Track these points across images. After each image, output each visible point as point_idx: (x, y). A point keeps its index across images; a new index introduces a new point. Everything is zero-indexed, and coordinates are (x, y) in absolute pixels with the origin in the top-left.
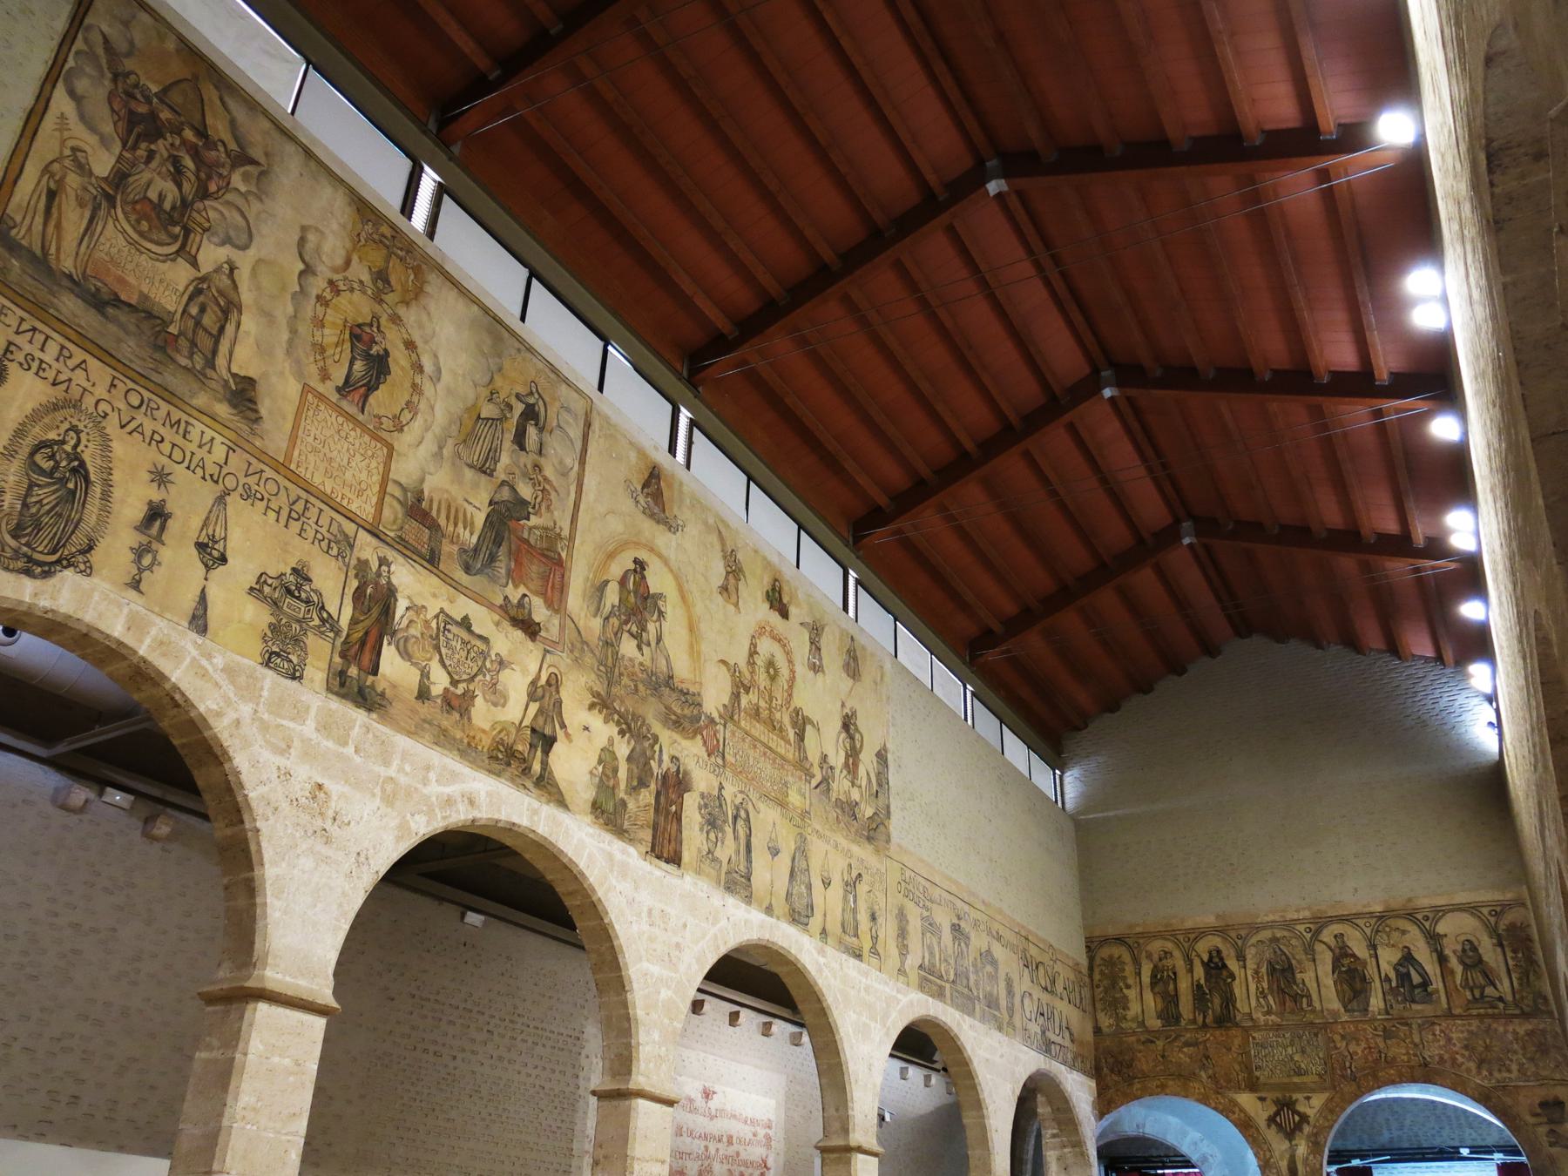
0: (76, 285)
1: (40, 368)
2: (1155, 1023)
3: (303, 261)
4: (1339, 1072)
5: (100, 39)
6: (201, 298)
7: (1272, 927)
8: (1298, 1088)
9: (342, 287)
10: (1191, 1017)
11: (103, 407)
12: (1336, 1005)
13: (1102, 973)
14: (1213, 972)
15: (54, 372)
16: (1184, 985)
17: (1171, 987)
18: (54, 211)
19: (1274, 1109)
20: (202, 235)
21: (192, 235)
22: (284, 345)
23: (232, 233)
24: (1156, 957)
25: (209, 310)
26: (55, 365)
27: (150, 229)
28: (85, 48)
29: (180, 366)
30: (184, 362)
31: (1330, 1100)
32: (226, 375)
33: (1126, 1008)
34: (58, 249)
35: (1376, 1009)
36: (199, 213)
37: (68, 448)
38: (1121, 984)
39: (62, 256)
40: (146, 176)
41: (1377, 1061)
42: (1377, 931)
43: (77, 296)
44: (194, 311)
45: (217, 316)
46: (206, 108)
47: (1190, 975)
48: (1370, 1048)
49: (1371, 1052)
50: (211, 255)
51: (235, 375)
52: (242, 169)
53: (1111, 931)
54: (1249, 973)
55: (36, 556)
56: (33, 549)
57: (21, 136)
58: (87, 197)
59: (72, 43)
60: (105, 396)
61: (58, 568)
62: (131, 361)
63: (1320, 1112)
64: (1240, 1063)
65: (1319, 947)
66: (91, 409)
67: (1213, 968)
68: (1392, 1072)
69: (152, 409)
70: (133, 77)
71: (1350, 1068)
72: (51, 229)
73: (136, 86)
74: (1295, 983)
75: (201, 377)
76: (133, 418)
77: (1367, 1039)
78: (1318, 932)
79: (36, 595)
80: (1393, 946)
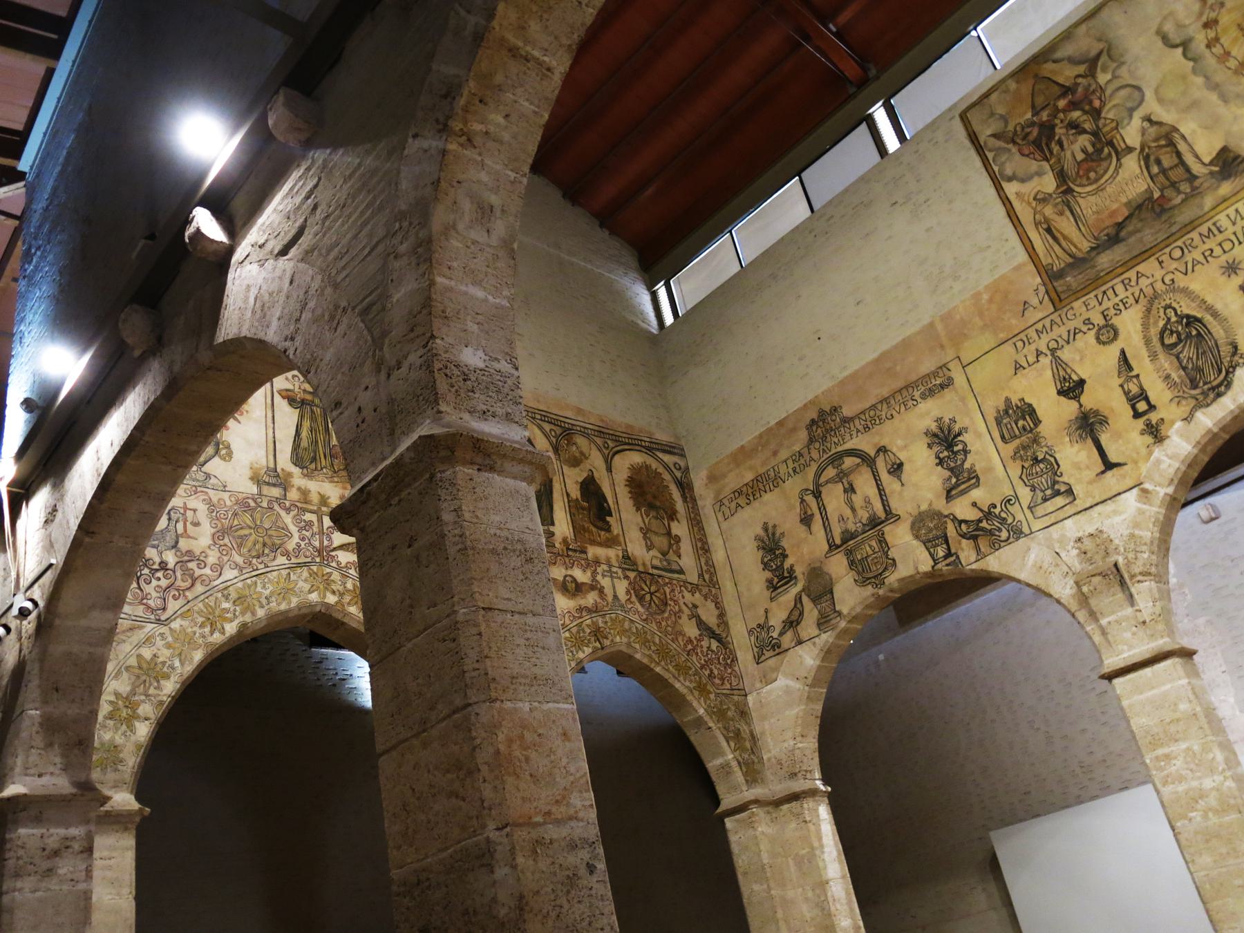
0: (1097, 249)
1: (1124, 304)
3: (1176, 46)
5: (992, 139)
6: (1152, 158)
9: (1213, 15)
11: (1167, 280)
15: (1131, 297)
18: (1058, 235)
20: (1118, 132)
21: (1115, 141)
22: (1219, 102)
23: (1129, 105)
25: (1162, 157)
26: (1129, 294)
27: (1096, 172)
28: (993, 154)
29: (1179, 204)
30: (1178, 200)
32: (1205, 170)
34: (1076, 247)
36: (1105, 125)
37: (1174, 319)
39: (1079, 246)
40: (1068, 154)
43: (1103, 251)
44: (1155, 169)
45: (1166, 153)
46: (1054, 78)
50: (1132, 134)
51: (1211, 163)
52: (1099, 69)
55: (1215, 383)
56: (1210, 382)
57: (1016, 228)
58: (1060, 207)
59: (988, 160)
60: (1163, 272)
61: (1231, 376)
62: (1156, 239)
66: (1164, 288)
69: (1190, 245)
70: (1018, 129)
72: (1064, 243)
73: (1023, 128)
75: (1195, 192)
76: (1186, 263)
79: (1234, 400)
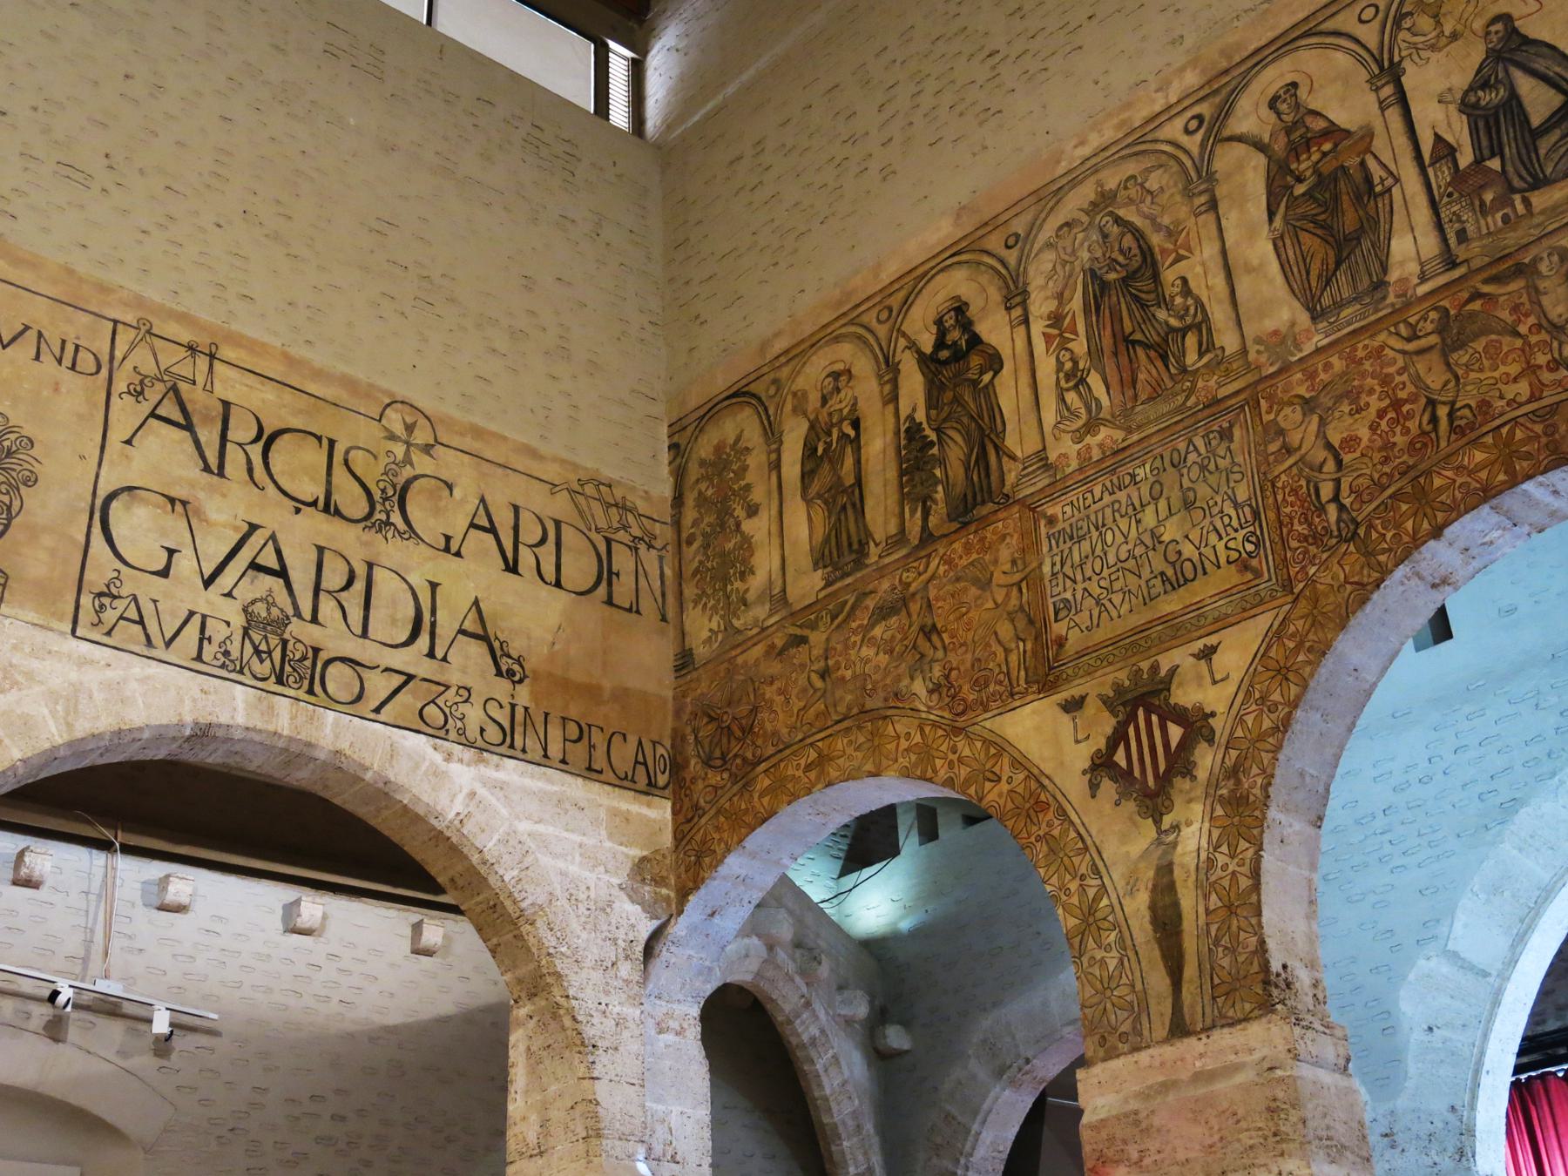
2: (807, 585)
4: (1300, 528)
7: (1095, 170)
8: (1174, 630)
10: (893, 529)
12: (1286, 312)
13: (702, 500)
14: (947, 372)
16: (878, 445)
17: (849, 462)
19: (1108, 724)
24: (814, 399)
31: (1276, 635)
33: (746, 572)
35: (1413, 268)
38: (739, 512)
41: (1422, 442)
42: (1399, 19)
47: (891, 407)
48: (1397, 404)
49: (1401, 419)
53: (721, 383)
54: (1037, 328)
63: (1247, 689)
64: (1011, 618)
65: (1227, 158)
67: (945, 363)
68: (1479, 456)
71: (1336, 498)
74: (1163, 301)
77: (1386, 381)
78: (1225, 111)
80: (1454, 36)
